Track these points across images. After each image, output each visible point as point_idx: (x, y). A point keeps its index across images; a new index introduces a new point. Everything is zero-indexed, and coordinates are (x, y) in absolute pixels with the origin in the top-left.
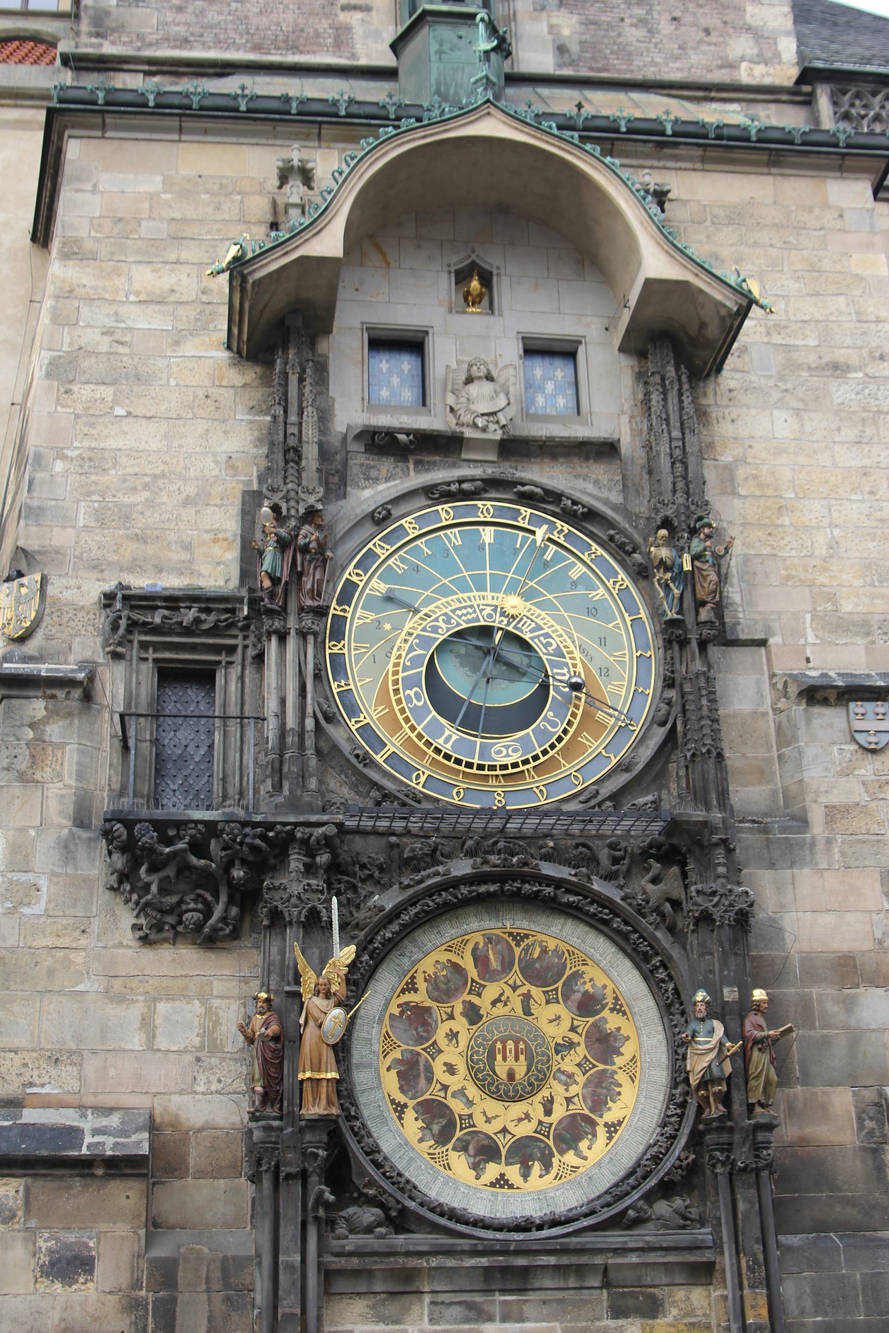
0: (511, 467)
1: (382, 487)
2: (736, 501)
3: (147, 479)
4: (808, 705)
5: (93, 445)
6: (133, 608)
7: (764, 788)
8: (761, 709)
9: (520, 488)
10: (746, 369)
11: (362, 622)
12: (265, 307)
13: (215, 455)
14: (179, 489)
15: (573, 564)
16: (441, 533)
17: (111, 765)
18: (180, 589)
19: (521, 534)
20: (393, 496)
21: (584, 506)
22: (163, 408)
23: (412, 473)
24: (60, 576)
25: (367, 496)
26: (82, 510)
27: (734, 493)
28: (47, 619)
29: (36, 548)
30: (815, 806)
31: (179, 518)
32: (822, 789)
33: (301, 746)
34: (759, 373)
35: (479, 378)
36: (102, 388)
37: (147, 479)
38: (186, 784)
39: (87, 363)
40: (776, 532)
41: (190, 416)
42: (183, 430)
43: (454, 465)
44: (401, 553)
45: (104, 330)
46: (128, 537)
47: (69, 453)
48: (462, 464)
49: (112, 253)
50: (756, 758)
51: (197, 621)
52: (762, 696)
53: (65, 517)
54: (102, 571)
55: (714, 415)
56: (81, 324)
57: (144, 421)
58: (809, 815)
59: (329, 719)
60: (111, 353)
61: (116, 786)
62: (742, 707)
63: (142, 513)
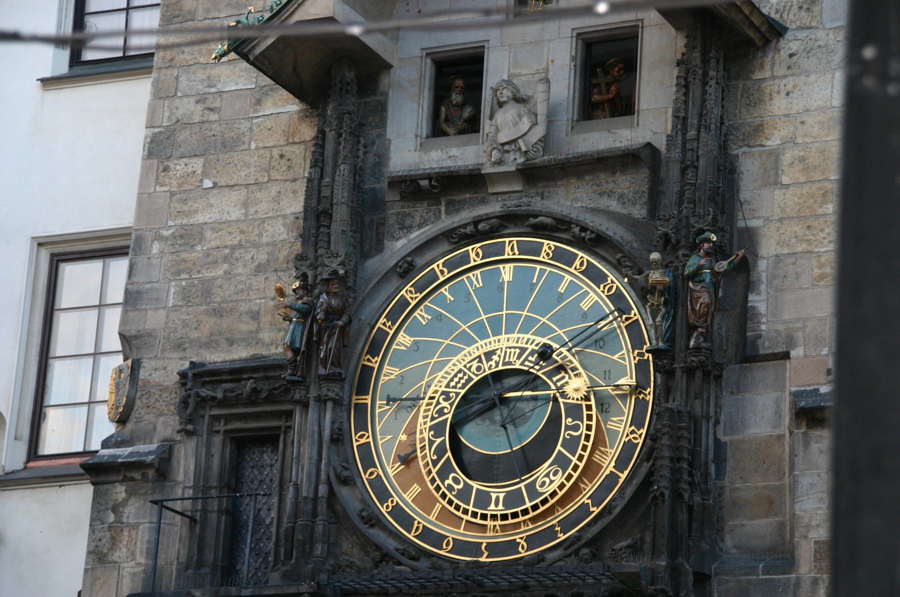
0: (537, 194)
1: (413, 235)
2: (777, 192)
3: (227, 251)
4: (808, 427)
5: (185, 221)
6: (204, 384)
7: (770, 520)
8: (777, 432)
9: (532, 221)
10: (813, 24)
11: (387, 378)
12: (295, 69)
13: (285, 217)
14: (252, 258)
15: (587, 293)
16: (464, 277)
17: (180, 539)
18: (246, 360)
19: (539, 267)
20: (413, 248)
21: (592, 232)
22: (243, 174)
23: (443, 216)
24: (151, 358)
25: (399, 246)
26: (173, 290)
27: (777, 183)
28: (138, 403)
29: (133, 333)
30: (804, 542)
31: (250, 288)
32: (814, 523)
33: (315, 514)
34: (828, 26)
35: (505, 102)
36: (195, 160)
37: (227, 251)
38: (257, 547)
39: (182, 136)
40: (815, 224)
41: (266, 179)
42: (259, 195)
43: (484, 201)
44: (426, 303)
45: (198, 97)
46: (207, 311)
47: (166, 233)
48: (492, 198)
49: (208, 11)
50: (765, 487)
51: (254, 391)
52: (780, 416)
53: (158, 299)
54: (185, 350)
55: (768, 91)
56: (179, 94)
57: (227, 190)
58: (796, 553)
59: (346, 481)
60: (203, 122)
61: (183, 559)
62: (759, 431)
63: (220, 286)
